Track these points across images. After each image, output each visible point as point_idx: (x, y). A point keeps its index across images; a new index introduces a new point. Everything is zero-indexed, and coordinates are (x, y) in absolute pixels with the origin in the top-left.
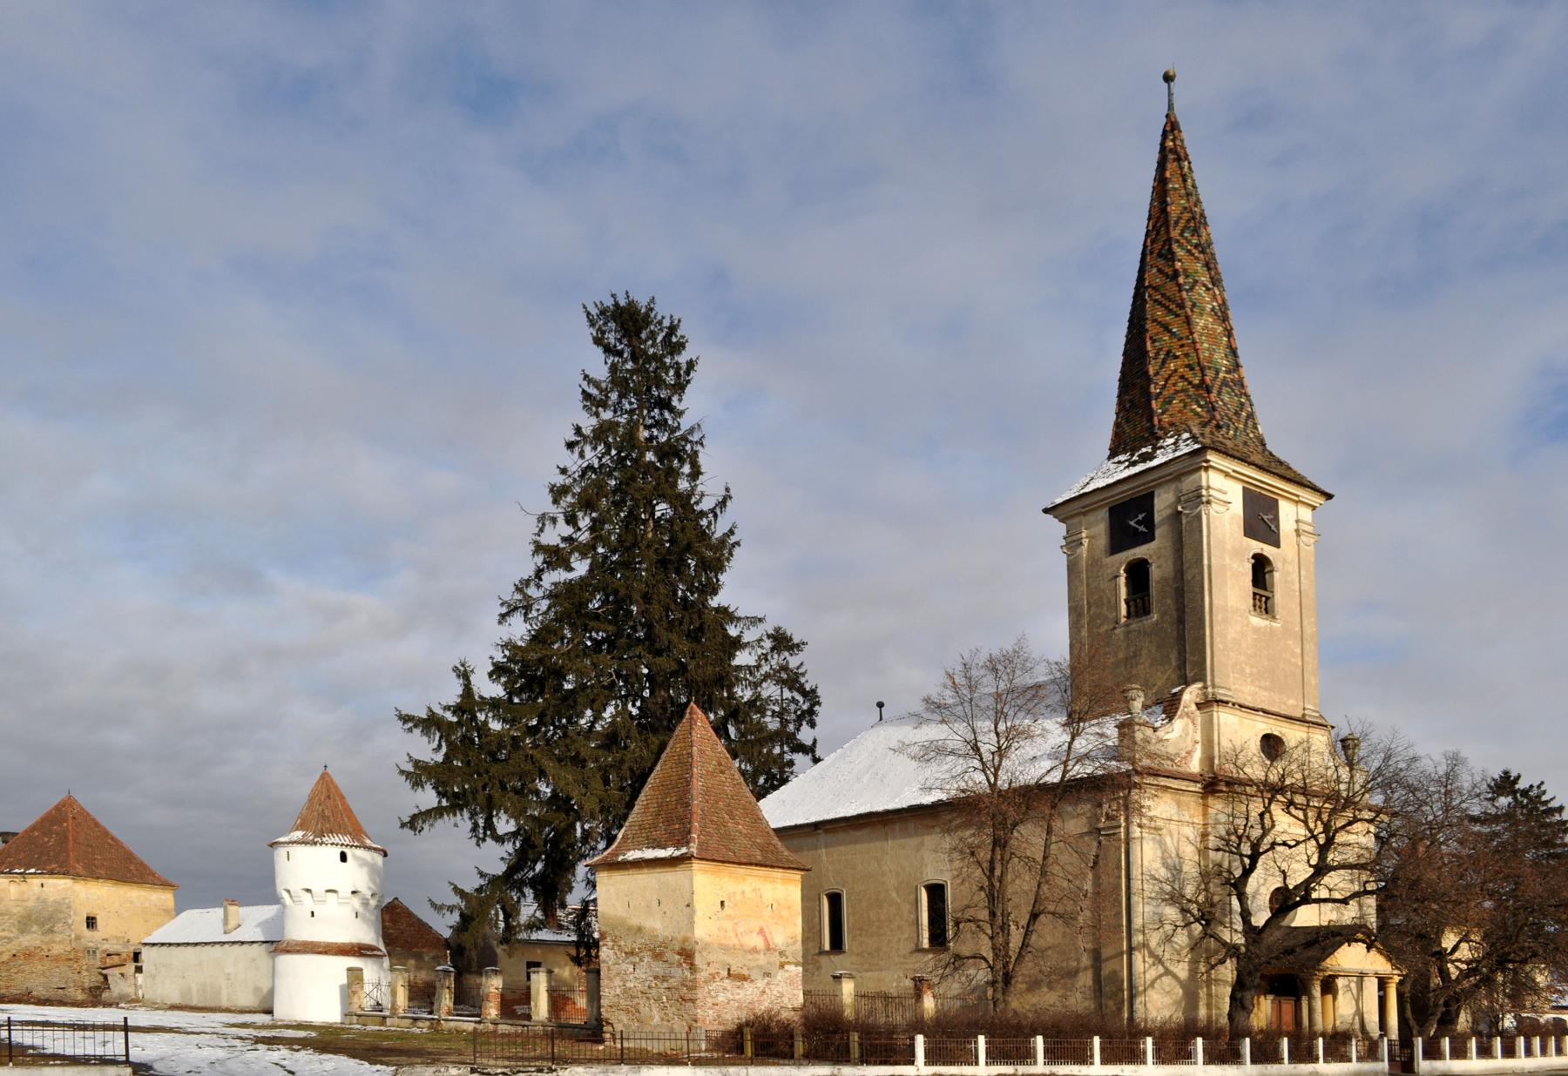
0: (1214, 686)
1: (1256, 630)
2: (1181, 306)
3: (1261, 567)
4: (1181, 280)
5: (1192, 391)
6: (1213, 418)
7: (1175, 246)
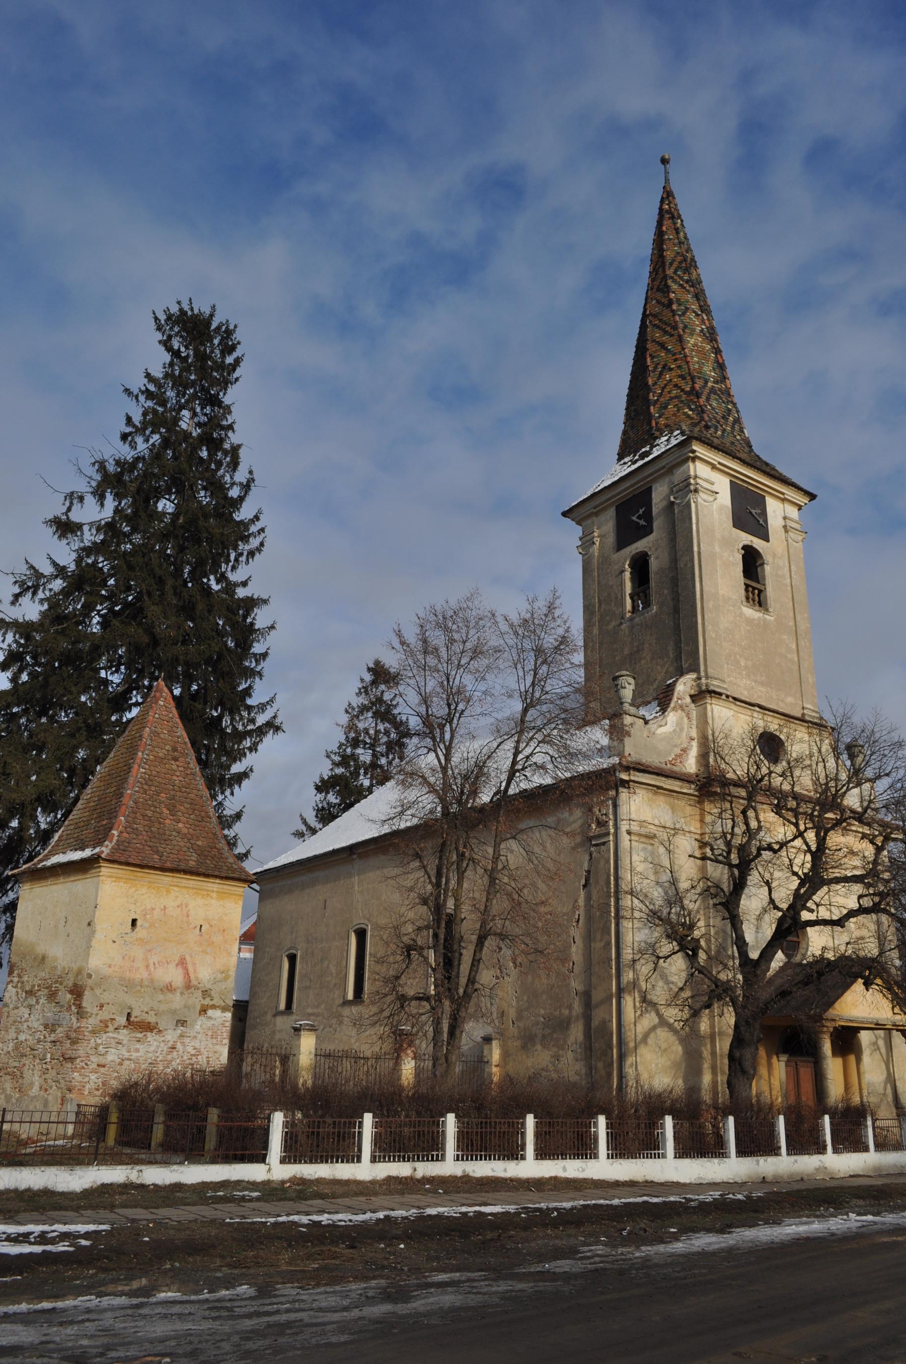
0: (707, 677)
1: (749, 621)
2: (675, 328)
3: (752, 562)
4: (674, 307)
5: (684, 397)
6: (702, 419)
7: (669, 282)
